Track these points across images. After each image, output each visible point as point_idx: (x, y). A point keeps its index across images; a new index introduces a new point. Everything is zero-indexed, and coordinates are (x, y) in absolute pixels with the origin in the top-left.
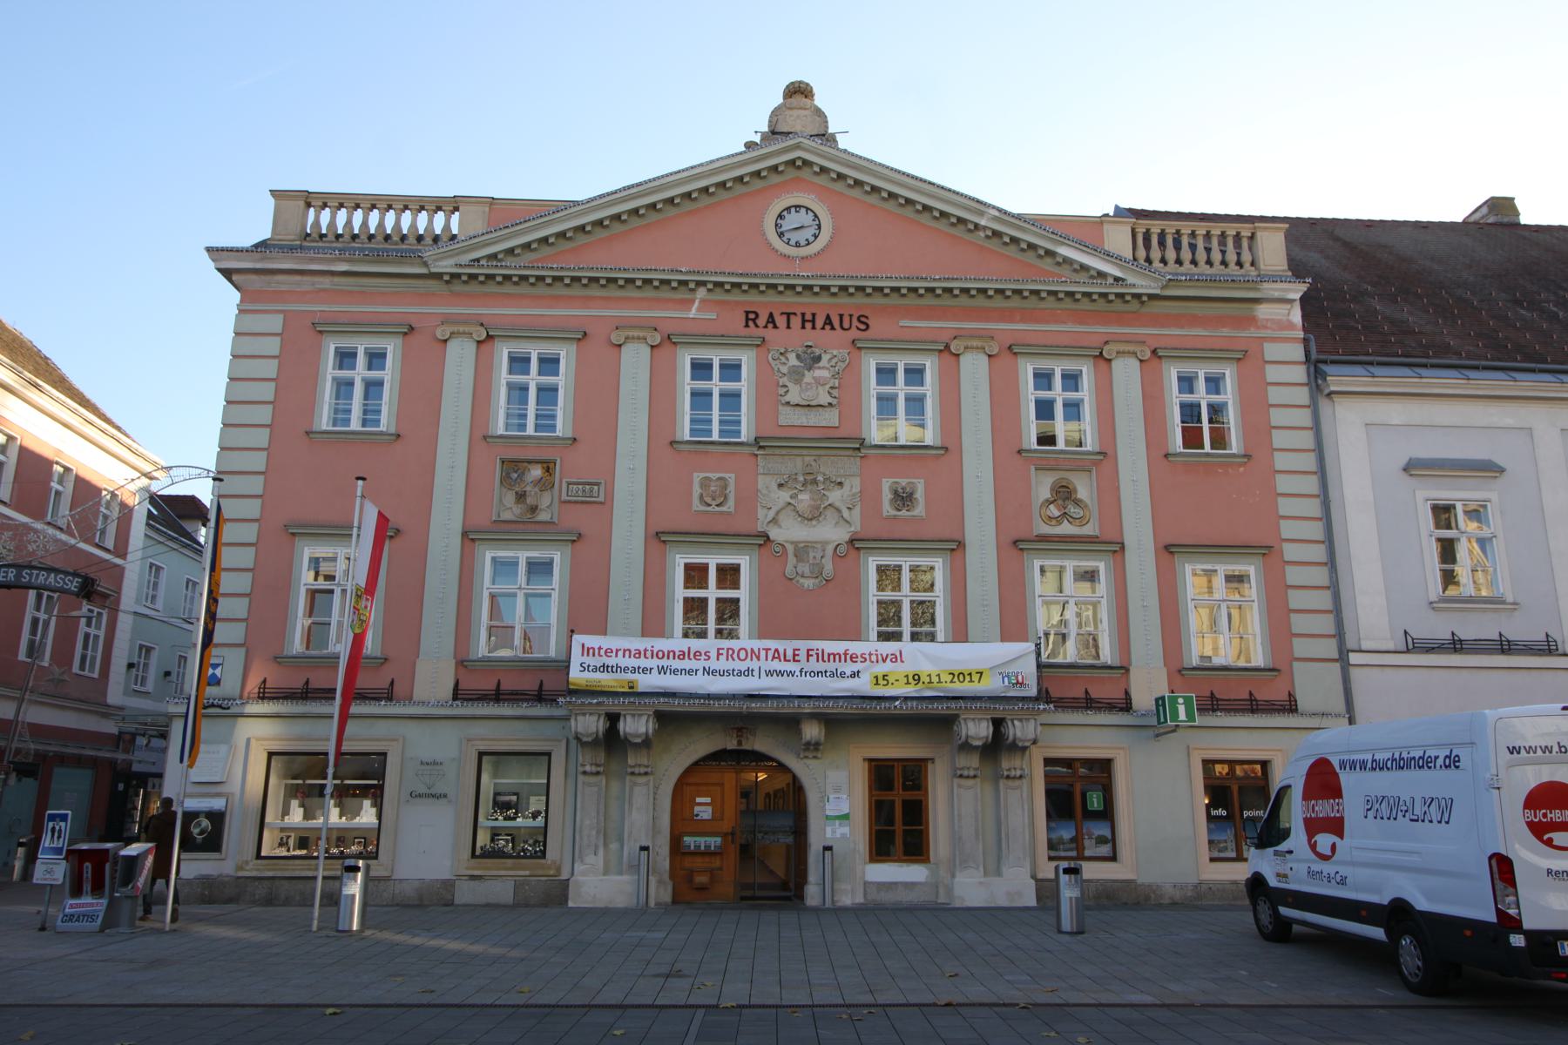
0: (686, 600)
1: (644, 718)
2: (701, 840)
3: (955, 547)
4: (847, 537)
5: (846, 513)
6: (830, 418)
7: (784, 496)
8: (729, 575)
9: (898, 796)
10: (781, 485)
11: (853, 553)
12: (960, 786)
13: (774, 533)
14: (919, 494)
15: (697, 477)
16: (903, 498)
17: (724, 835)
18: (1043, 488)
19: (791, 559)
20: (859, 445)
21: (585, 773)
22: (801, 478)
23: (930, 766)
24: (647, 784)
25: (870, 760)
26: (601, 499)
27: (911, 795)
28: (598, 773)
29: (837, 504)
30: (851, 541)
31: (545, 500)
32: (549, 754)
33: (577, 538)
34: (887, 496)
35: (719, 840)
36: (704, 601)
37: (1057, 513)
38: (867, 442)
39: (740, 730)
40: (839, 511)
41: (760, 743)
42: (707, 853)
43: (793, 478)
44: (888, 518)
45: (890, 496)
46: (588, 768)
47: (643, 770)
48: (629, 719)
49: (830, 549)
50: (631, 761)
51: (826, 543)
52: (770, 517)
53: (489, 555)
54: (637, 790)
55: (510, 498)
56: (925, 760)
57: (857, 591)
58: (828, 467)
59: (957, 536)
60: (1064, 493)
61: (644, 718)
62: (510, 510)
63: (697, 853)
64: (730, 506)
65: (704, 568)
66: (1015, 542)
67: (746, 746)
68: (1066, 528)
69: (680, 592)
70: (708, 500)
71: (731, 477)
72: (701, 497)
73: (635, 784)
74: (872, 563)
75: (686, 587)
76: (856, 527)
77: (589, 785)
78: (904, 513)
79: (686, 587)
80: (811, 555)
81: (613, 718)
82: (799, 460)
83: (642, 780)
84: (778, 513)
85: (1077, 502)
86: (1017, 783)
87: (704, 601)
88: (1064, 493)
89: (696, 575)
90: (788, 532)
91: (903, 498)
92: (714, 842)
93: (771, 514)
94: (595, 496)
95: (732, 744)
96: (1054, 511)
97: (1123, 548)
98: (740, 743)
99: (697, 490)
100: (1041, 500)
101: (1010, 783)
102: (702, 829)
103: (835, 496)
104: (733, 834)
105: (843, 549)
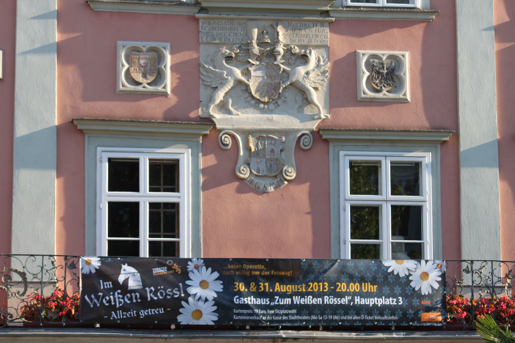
8: (166, 175)
36: (135, 206)
65: (134, 165)
70: (139, 77)
72: (128, 72)
87: (135, 206)
89: (123, 175)
105: (307, 141)
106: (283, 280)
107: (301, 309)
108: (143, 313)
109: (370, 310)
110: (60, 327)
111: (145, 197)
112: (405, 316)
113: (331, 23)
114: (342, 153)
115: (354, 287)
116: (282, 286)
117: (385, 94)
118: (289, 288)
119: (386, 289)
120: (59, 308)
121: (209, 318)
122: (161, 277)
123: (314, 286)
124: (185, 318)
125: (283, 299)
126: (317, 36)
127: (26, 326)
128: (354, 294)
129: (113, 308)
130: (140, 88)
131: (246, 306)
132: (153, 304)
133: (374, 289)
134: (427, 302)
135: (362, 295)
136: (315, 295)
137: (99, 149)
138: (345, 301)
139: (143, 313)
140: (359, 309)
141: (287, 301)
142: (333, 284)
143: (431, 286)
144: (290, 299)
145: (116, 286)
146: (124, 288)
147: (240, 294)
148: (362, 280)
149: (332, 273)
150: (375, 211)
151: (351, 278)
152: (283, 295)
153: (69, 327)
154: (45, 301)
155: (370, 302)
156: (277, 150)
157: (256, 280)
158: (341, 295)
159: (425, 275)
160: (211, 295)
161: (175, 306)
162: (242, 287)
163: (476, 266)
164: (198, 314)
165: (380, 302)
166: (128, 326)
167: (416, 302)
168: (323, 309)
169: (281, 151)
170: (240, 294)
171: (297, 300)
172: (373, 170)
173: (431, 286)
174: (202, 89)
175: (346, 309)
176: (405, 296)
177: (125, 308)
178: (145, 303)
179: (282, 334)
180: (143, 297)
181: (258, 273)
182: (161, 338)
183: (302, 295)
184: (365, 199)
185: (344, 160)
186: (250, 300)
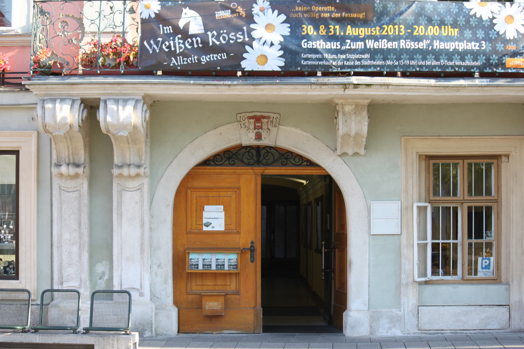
2: (213, 259)
9: (463, 201)
17: (242, 252)
21: (61, 175)
23: (504, 166)
24: (140, 189)
27: (481, 201)
28: (76, 176)
32: (16, 153)
35: (234, 257)
42: (220, 275)
48: (112, 106)
50: (117, 160)
54: (127, 196)
56: (497, 157)
63: (206, 275)
67: (266, 141)
81: (91, 107)
83: (132, 184)
92: (229, 259)
95: (248, 139)
98: (259, 137)
102: (213, 243)
104: (252, 250)
106: (354, 22)
107: (374, 53)
108: (204, 59)
109: (450, 55)
110: (119, 74)
112: (488, 63)
115: (433, 31)
116: (354, 29)
118: (362, 31)
119: (468, 33)
120: (117, 54)
121: (275, 63)
122: (226, 21)
123: (390, 30)
124: (249, 63)
125: (355, 43)
127: (85, 74)
128: (434, 38)
129: (172, 54)
131: (315, 51)
132: (215, 49)
133: (455, 32)
134: (512, 47)
135: (441, 39)
136: (389, 39)
138: (423, 45)
139: (204, 59)
140: (437, 54)
141: (360, 45)
142: (410, 27)
143: (517, 30)
144: (363, 43)
145: (177, 30)
146: (185, 34)
147: (308, 37)
148: (442, 23)
149: (408, 16)
151: (430, 21)
152: (356, 39)
153: (126, 74)
154: (103, 48)
155: (451, 46)
157: (325, 22)
158: (418, 39)
159: (510, 19)
160: (277, 38)
161: (238, 51)
162: (310, 30)
164: (264, 58)
165: (462, 46)
166: (190, 73)
167: (500, 47)
168: (399, 53)
170: (308, 37)
171: (371, 44)
173: (517, 30)
175: (424, 54)
176: (487, 39)
177: (184, 54)
178: (206, 48)
179: (355, 80)
180: (205, 43)
181: (328, 14)
182: (223, 85)
183: (376, 39)
186: (320, 44)
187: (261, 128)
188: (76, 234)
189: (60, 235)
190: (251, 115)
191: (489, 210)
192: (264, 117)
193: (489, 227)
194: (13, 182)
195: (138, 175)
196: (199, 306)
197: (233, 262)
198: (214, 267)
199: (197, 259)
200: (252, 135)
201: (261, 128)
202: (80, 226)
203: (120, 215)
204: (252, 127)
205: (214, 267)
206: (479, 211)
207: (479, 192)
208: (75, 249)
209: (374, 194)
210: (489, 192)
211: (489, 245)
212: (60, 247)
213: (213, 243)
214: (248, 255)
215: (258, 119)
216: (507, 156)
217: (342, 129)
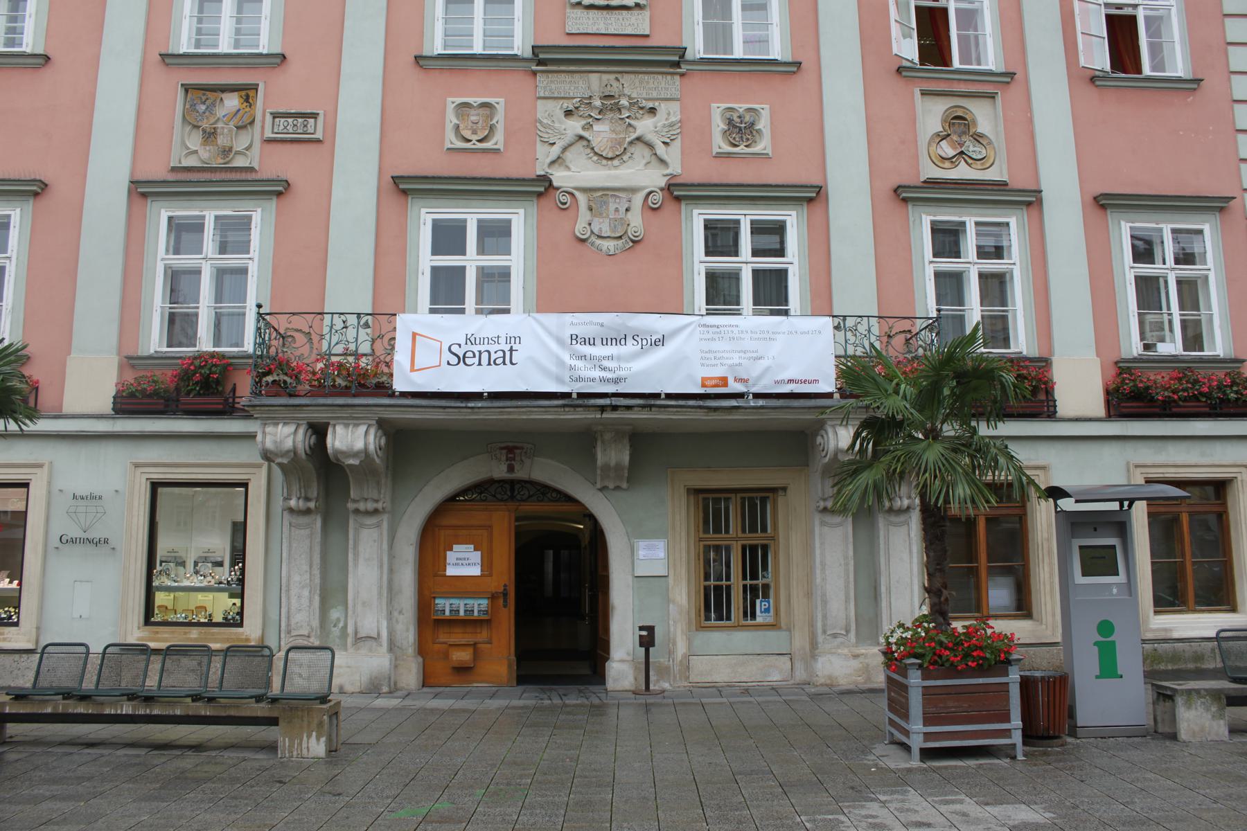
0: (435, 271)
1: (363, 429)
2: (461, 605)
3: (812, 196)
4: (662, 182)
5: (661, 150)
6: (636, 23)
7: (574, 126)
8: (494, 235)
10: (568, 113)
11: (671, 207)
12: (823, 524)
13: (560, 177)
14: (763, 124)
15: (452, 101)
16: (741, 129)
17: (493, 597)
18: (932, 115)
19: (584, 215)
20: (673, 61)
21: (291, 510)
22: (597, 103)
23: (781, 500)
24: (378, 526)
25: (696, 492)
26: (319, 135)
27: (756, 539)
28: (308, 512)
29: (651, 137)
30: (669, 188)
31: (241, 142)
32: (245, 485)
33: (279, 190)
34: (719, 125)
35: (484, 602)
37: (951, 152)
38: (689, 55)
39: (510, 450)
40: (650, 146)
41: (545, 471)
42: (469, 623)
43: (587, 101)
44: (720, 156)
45: (723, 126)
46: (293, 503)
47: (370, 506)
49: (638, 199)
51: (634, 190)
52: (553, 157)
53: (164, 215)
55: (195, 141)
57: (679, 257)
58: (634, 87)
59: (815, 180)
60: (958, 123)
61: (363, 429)
62: (189, 150)
64: (497, 141)
65: (461, 227)
66: (896, 190)
67: (520, 474)
68: (963, 172)
69: (425, 259)
71: (499, 102)
72: (457, 127)
73: (362, 526)
74: (697, 219)
75: (434, 253)
76: (675, 167)
77: (298, 527)
78: (741, 149)
79: (434, 253)
80: (612, 207)
81: (319, 431)
82: (594, 77)
84: (565, 149)
85: (978, 138)
86: (902, 518)
88: (958, 123)
90: (577, 173)
91: (741, 129)
92: (479, 605)
93: (555, 151)
94: (305, 131)
95: (499, 471)
96: (947, 150)
97: (1040, 202)
98: (511, 469)
99: (451, 119)
100: (928, 137)
101: (893, 519)
103: (645, 126)
104: (505, 595)
111: (472, 261)
113: (682, 75)
114: (696, 212)
117: (741, 149)
126: (667, 89)
130: (468, 145)
137: (424, 211)
150: (735, 276)
156: (623, 210)
163: (850, 322)
169: (627, 210)
172: (732, 228)
174: (539, 145)
184: (722, 263)
185: (697, 219)
187: (514, 459)
188: (307, 576)
189: (289, 577)
190: (503, 445)
191: (765, 548)
192: (517, 448)
193: (765, 568)
194: (242, 519)
195: (376, 511)
196: (446, 656)
197: (484, 607)
198: (462, 613)
199: (445, 605)
200: (504, 468)
201: (514, 459)
202: (311, 567)
203: (356, 555)
204: (504, 458)
205: (462, 613)
206: (753, 549)
207: (753, 529)
208: (306, 593)
209: (638, 531)
210: (764, 529)
211: (766, 587)
212: (288, 591)
213: (462, 587)
214: (501, 601)
215: (510, 450)
216: (784, 489)
217: (601, 458)
